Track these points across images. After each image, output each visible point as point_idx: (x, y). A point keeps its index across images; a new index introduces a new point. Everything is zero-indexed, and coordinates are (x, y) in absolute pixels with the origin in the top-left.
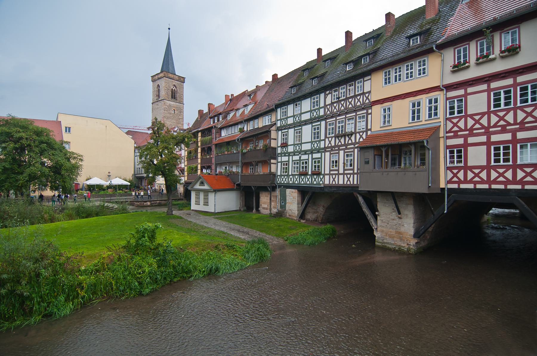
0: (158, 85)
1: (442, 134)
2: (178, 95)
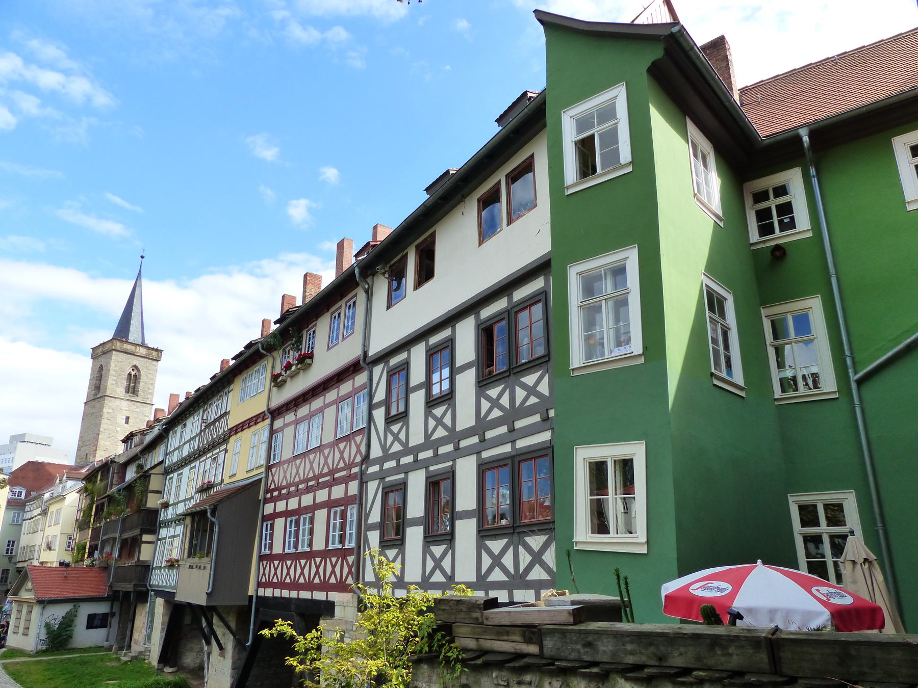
0: (102, 365)
2: (141, 385)
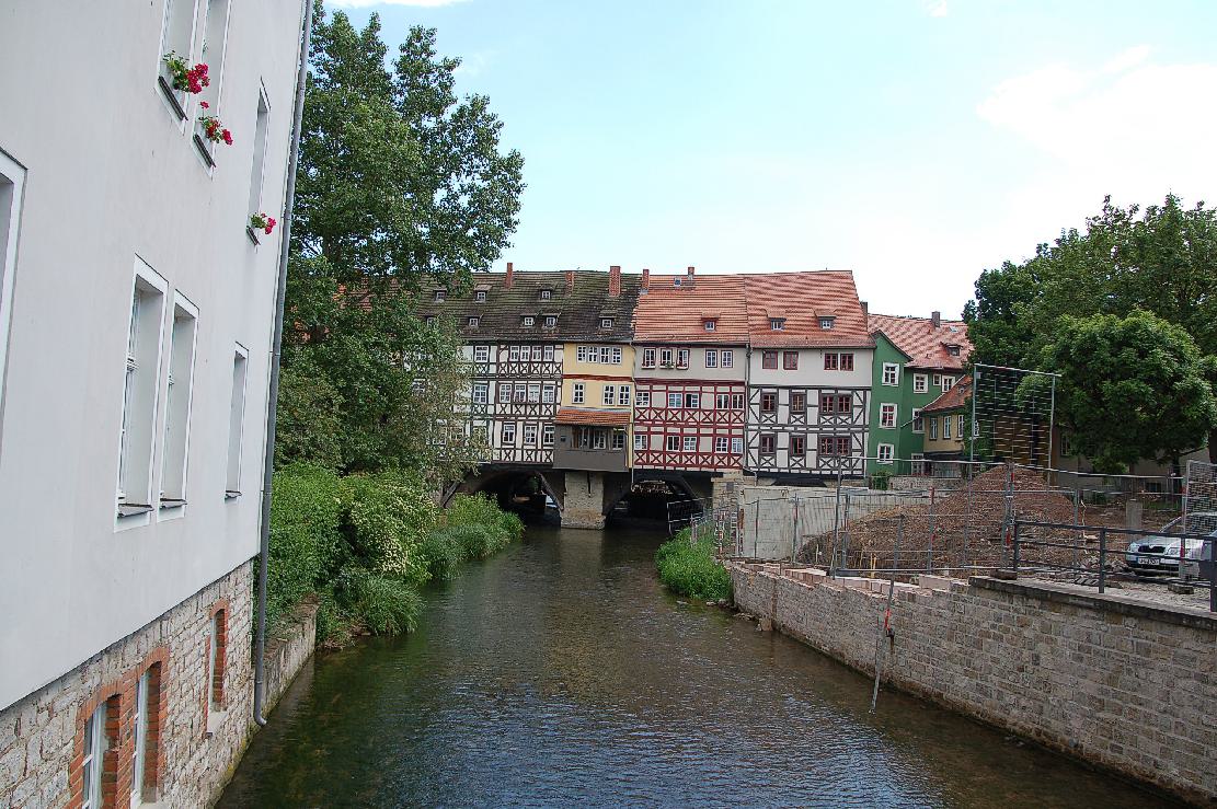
1: (632, 420)
